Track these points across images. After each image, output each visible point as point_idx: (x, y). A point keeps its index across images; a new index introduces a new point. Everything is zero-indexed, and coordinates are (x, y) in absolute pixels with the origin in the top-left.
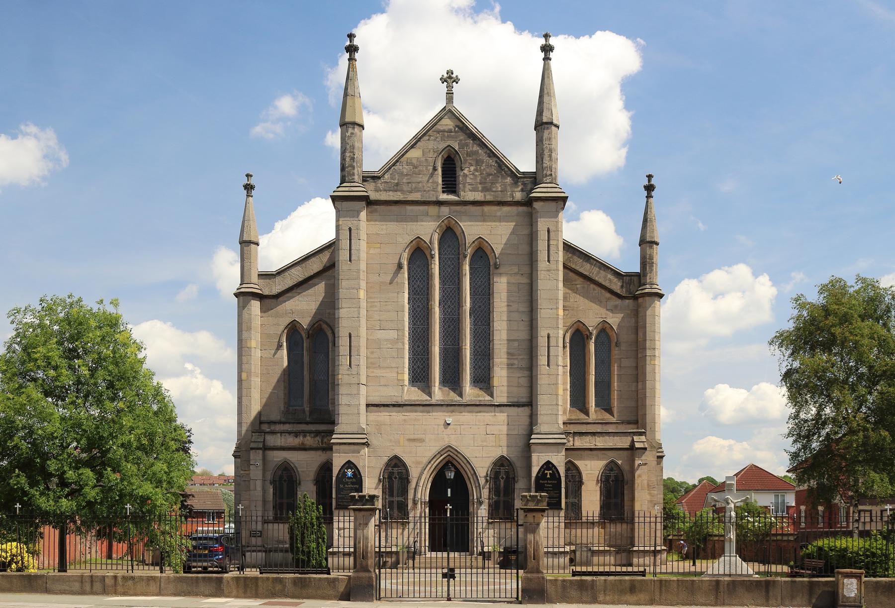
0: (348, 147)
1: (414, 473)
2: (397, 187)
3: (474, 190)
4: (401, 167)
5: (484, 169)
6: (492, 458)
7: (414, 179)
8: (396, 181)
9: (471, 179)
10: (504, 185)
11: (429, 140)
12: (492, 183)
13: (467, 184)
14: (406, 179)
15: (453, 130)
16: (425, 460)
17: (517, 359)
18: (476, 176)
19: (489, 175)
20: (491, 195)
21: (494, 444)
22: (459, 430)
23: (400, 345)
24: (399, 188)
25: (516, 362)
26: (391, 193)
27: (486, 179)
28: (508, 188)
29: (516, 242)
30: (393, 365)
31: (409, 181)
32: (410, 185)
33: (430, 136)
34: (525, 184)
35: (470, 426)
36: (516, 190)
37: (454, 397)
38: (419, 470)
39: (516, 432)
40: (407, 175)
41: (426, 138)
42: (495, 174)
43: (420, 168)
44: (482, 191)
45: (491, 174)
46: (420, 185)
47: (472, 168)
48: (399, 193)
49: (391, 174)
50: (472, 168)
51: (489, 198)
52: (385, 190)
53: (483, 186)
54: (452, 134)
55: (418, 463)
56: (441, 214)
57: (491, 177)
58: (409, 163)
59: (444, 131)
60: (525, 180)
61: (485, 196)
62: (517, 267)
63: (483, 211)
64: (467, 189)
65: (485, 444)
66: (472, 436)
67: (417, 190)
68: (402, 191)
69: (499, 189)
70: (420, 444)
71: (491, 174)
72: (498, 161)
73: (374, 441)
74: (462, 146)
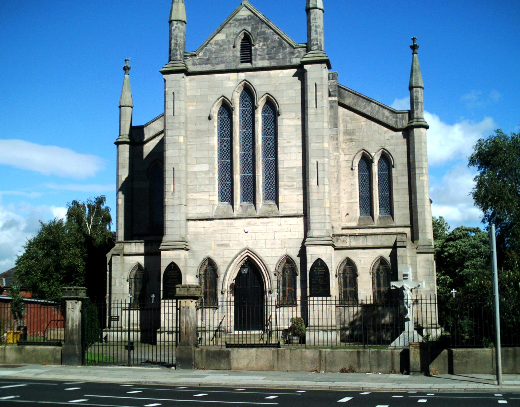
0: (173, 37)
1: (221, 270)
2: (208, 61)
3: (263, 59)
4: (211, 47)
5: (270, 44)
6: (278, 258)
7: (221, 55)
8: (207, 57)
9: (260, 51)
10: (285, 54)
11: (230, 27)
12: (275, 53)
13: (257, 55)
14: (215, 55)
15: (247, 19)
16: (230, 260)
17: (296, 181)
18: (264, 49)
19: (273, 47)
20: (275, 62)
21: (280, 246)
22: (254, 236)
23: (211, 175)
24: (209, 62)
25: (295, 184)
26: (204, 66)
27: (271, 51)
28: (288, 56)
29: (294, 95)
30: (206, 190)
31: (216, 56)
32: (217, 59)
33: (231, 24)
34: (300, 52)
35: (262, 233)
36: (293, 57)
37: (251, 210)
38: (226, 268)
39: (297, 237)
40: (215, 52)
41: (228, 25)
42: (278, 46)
43: (224, 46)
44: (268, 60)
45: (275, 47)
46: (224, 58)
47: (261, 44)
48: (209, 65)
49: (204, 53)
50: (261, 44)
51: (274, 64)
52: (200, 64)
53: (269, 56)
54: (247, 21)
55: (225, 262)
56: (239, 78)
57: (274, 49)
58: (217, 43)
59: (241, 20)
60: (300, 49)
61: (270, 63)
62: (294, 113)
63: (269, 74)
64: (257, 59)
65: (273, 246)
66: (264, 241)
67: (222, 62)
68: (212, 64)
69: (281, 57)
70: (227, 248)
71: (275, 47)
72: (280, 37)
73: (193, 247)
74: (253, 29)
